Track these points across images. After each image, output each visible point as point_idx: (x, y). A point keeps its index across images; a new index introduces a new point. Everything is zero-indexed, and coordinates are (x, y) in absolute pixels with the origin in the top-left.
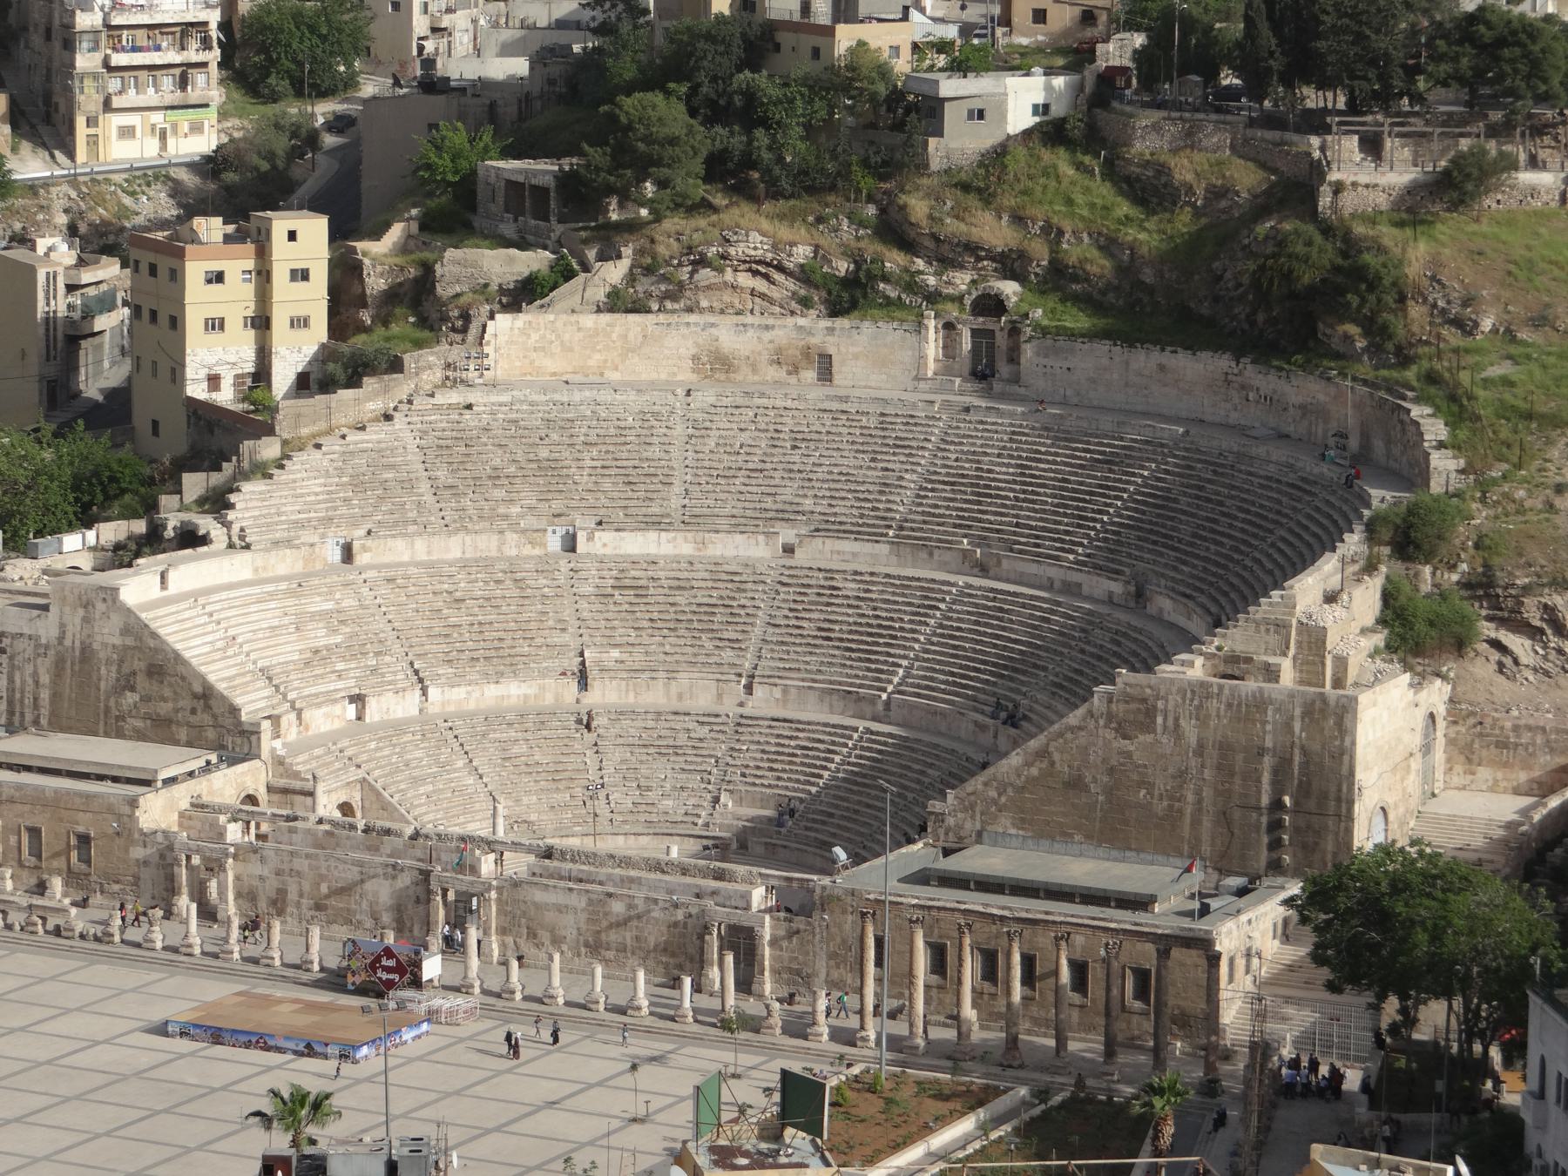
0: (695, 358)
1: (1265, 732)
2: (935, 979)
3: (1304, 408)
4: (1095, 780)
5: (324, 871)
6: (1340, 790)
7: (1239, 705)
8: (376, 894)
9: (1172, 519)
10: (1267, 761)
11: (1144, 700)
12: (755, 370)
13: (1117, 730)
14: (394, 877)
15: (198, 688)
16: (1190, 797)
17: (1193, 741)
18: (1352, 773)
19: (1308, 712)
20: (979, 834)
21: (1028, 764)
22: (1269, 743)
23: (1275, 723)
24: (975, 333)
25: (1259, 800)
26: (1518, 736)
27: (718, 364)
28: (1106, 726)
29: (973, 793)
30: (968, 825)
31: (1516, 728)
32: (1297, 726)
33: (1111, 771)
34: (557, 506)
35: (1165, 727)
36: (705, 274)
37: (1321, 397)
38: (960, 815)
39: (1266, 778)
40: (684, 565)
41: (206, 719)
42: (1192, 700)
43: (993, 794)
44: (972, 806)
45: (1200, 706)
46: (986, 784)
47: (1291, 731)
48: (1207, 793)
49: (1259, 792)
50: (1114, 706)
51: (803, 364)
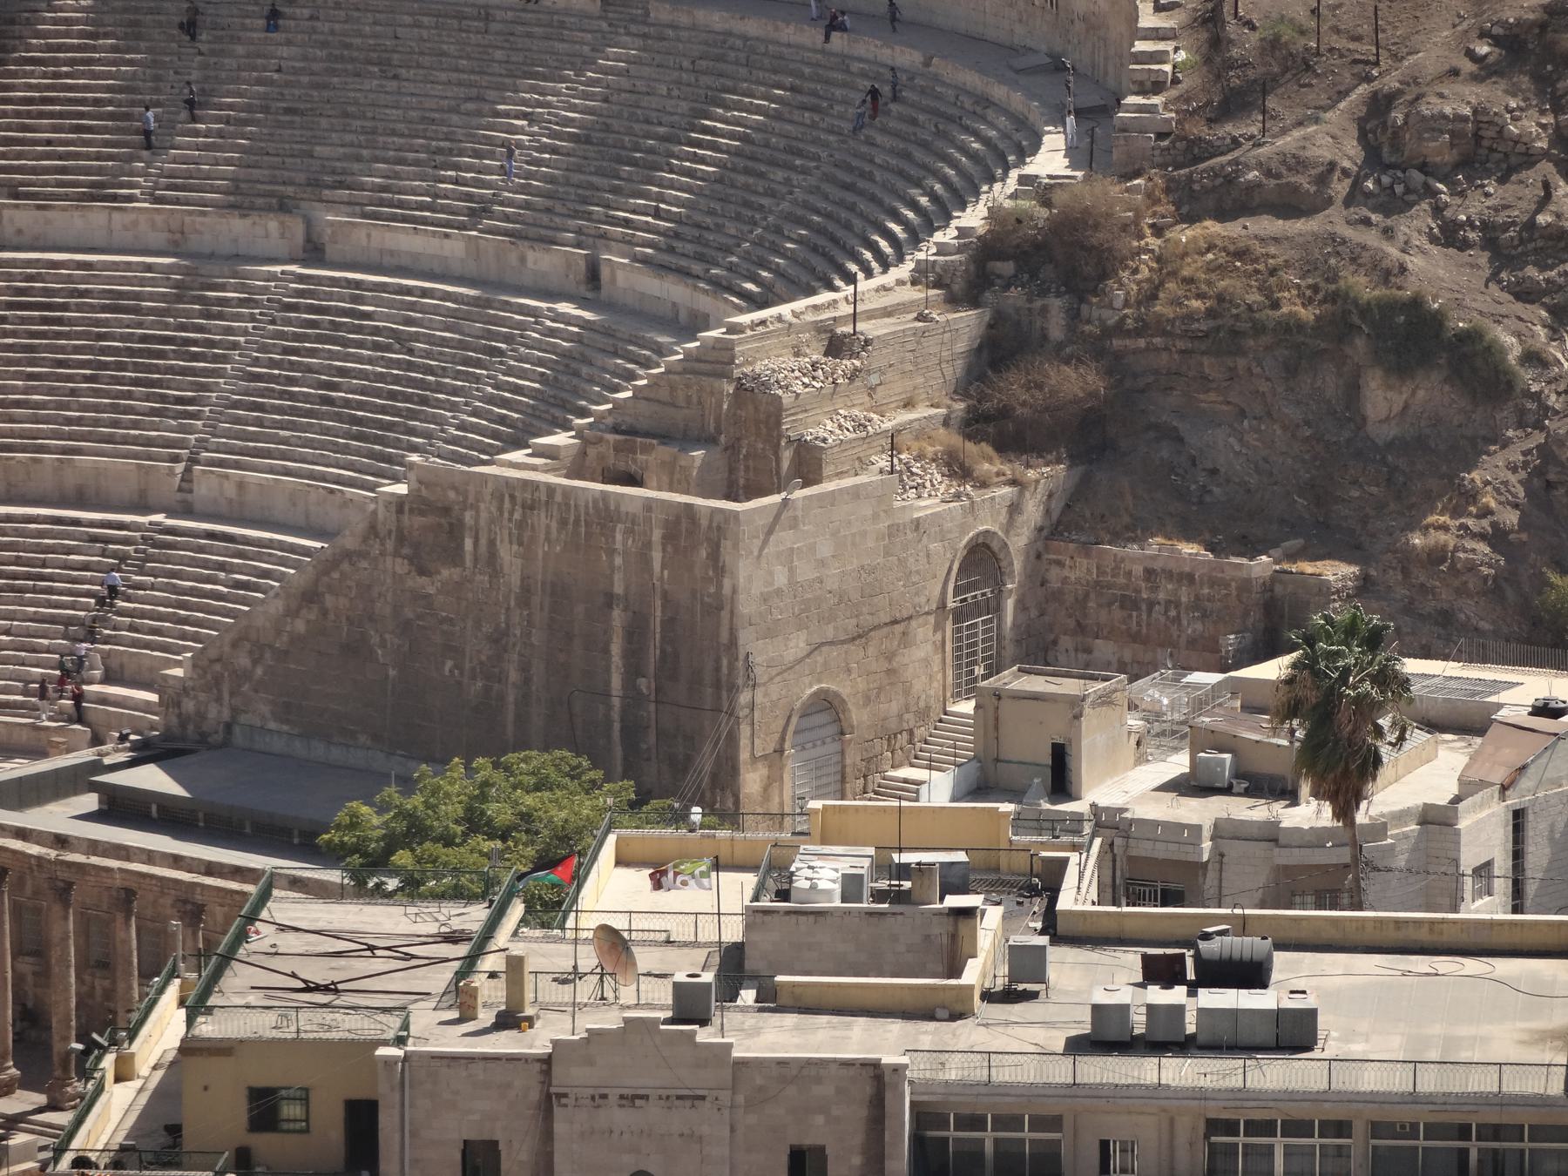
1: (612, 568)
2: (27, 965)
4: (383, 645)
6: (718, 669)
7: (577, 522)
9: (852, 208)
10: (618, 617)
11: (446, 511)
13: (411, 560)
16: (514, 676)
17: (515, 580)
18: (733, 642)
19: (670, 537)
20: (229, 727)
21: (291, 613)
22: (618, 589)
23: (625, 553)
25: (608, 683)
26: (1154, 589)
28: (396, 554)
29: (218, 660)
30: (213, 712)
31: (1150, 573)
32: (657, 556)
33: (405, 627)
35: (476, 560)
38: (202, 696)
39: (616, 649)
42: (511, 513)
43: (244, 661)
44: (218, 681)
45: (521, 525)
47: (650, 571)
48: (538, 668)
49: (608, 670)
50: (406, 518)
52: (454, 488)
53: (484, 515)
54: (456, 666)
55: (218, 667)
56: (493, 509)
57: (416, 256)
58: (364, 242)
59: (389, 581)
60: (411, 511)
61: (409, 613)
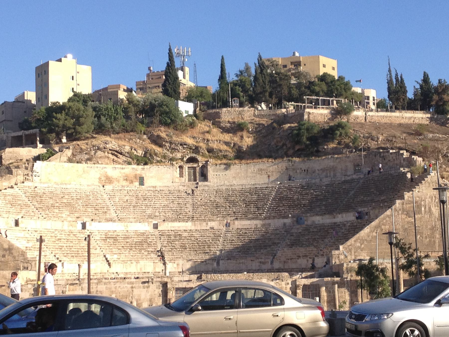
0: (100, 179)
3: (323, 170)
5: (113, 289)
8: (139, 296)
12: (118, 181)
13: (406, 215)
14: (148, 287)
15: (6, 246)
24: (188, 167)
27: (109, 180)
29: (350, 245)
34: (77, 215)
36: (99, 153)
37: (332, 164)
40: (126, 232)
41: (10, 258)
43: (358, 244)
46: (355, 241)
50: (405, 205)
51: (135, 180)
52: (418, 197)
53: (427, 202)
54: (421, 236)
55: (350, 247)
56: (430, 200)
57: (179, 227)
58: (167, 225)
59: (400, 220)
60: (406, 204)
61: (406, 227)
